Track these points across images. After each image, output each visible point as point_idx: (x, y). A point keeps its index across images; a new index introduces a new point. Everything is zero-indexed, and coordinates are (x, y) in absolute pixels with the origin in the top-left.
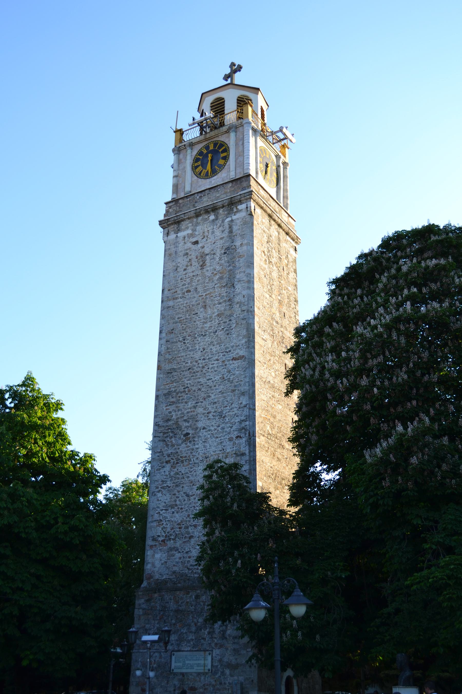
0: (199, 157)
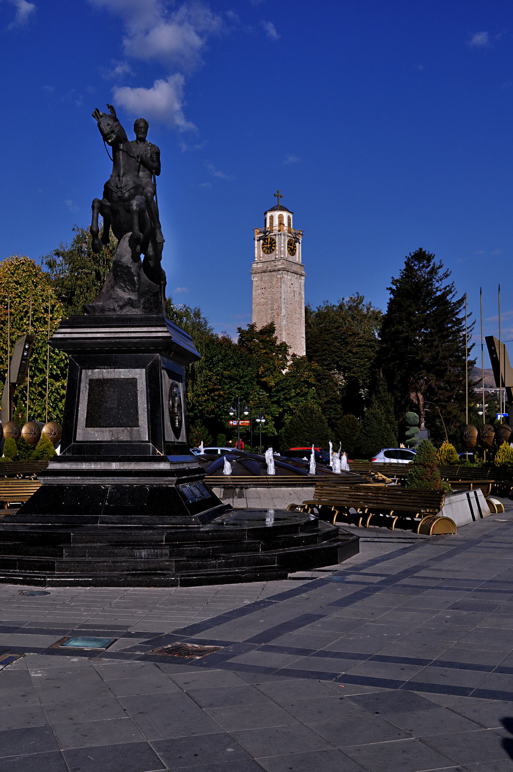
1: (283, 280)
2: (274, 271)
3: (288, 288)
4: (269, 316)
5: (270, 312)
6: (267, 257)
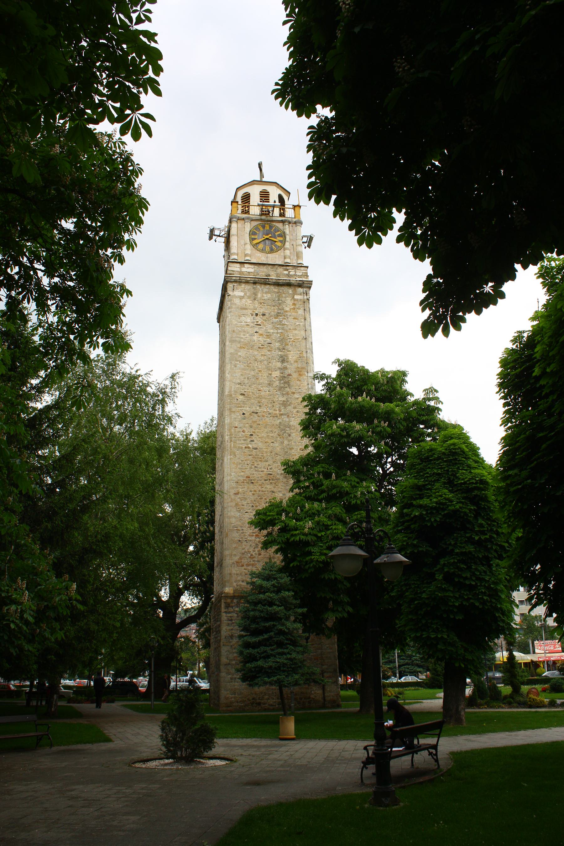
4: (277, 374)
5: (279, 365)
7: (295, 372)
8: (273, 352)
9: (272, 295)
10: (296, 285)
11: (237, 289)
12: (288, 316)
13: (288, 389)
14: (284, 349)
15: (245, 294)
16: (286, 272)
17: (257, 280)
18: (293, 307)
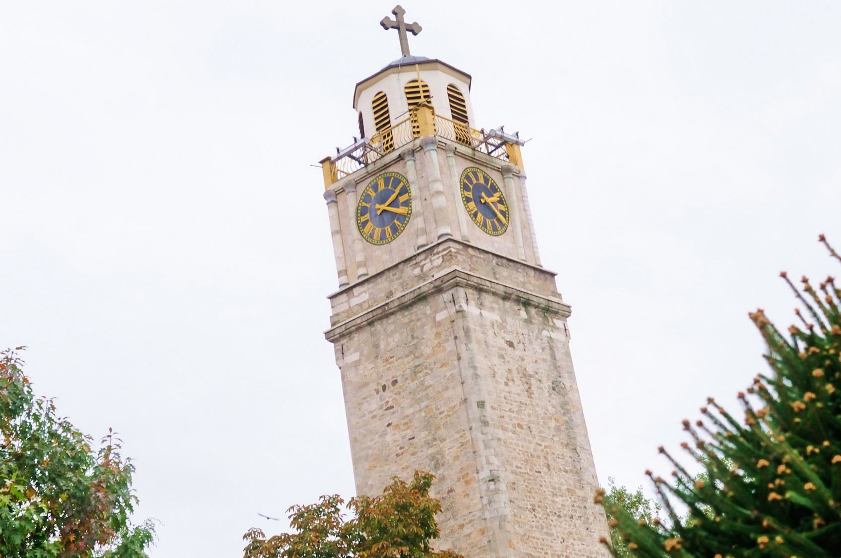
0: (364, 204)
1: (459, 323)
2: (421, 298)
3: (496, 360)
6: (386, 257)
7: (459, 480)
8: (419, 454)
9: (401, 334)
10: (432, 293)
11: (348, 350)
12: (432, 366)
13: (451, 523)
14: (435, 439)
15: (361, 355)
16: (417, 271)
17: (371, 315)
18: (436, 342)
